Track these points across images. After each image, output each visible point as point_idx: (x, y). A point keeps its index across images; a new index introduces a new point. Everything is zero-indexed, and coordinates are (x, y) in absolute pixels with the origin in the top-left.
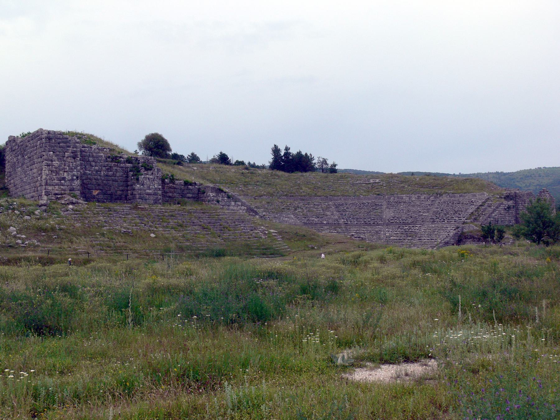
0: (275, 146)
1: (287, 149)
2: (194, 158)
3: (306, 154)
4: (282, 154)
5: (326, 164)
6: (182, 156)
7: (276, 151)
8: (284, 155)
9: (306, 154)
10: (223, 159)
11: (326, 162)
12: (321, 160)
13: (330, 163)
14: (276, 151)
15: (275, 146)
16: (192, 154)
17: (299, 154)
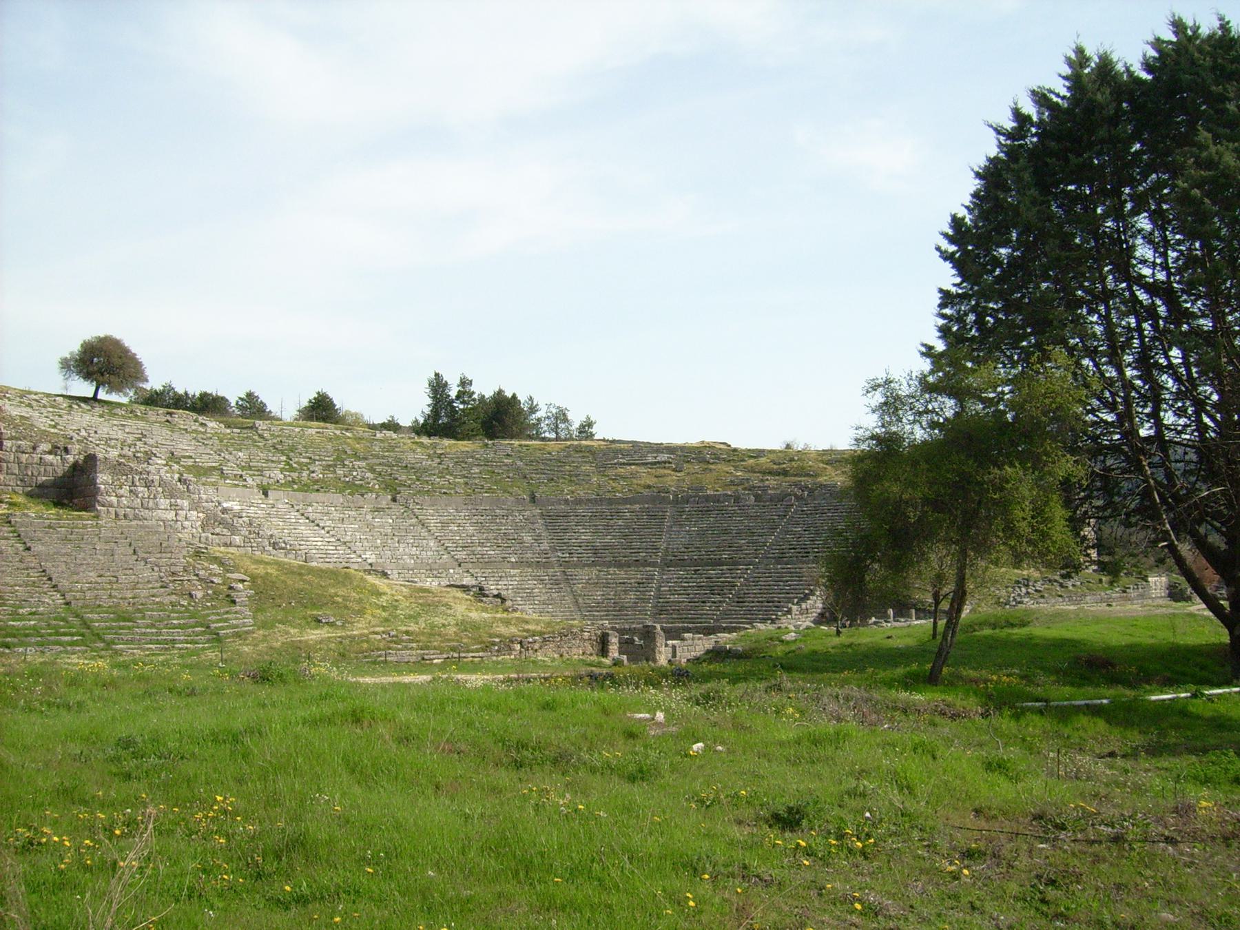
0: (437, 375)
1: (464, 383)
2: (253, 408)
3: (514, 396)
4: (453, 394)
5: (565, 420)
6: (223, 400)
7: (438, 387)
8: (458, 397)
9: (514, 396)
10: (321, 409)
11: (564, 415)
12: (554, 411)
13: (576, 419)
14: (438, 387)
15: (437, 375)
16: (250, 395)
17: (499, 397)
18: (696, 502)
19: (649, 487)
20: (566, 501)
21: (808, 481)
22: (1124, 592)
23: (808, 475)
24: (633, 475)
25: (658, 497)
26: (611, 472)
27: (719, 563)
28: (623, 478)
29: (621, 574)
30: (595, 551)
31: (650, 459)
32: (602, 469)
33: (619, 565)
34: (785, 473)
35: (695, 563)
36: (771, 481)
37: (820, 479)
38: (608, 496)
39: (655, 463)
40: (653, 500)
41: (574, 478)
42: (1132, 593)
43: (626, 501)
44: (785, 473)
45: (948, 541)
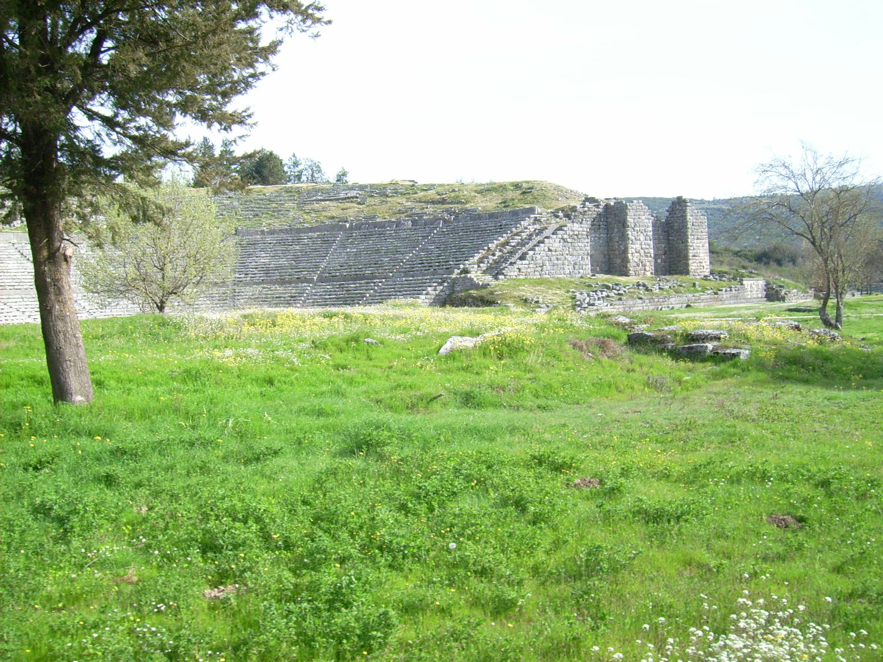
4: (217, 153)
18: (369, 228)
19: (333, 218)
20: (263, 232)
21: (456, 207)
22: (716, 293)
23: (460, 203)
24: (324, 209)
25: (337, 225)
26: (308, 207)
27: (363, 277)
28: (315, 211)
29: (280, 289)
30: (267, 272)
31: (342, 196)
32: (301, 206)
33: (282, 282)
34: (443, 202)
35: (345, 278)
36: (430, 209)
37: (468, 206)
38: (299, 226)
39: (345, 199)
40: (332, 228)
41: (277, 213)
42: (724, 295)
43: (311, 230)
44: (443, 202)
45: (80, 188)
